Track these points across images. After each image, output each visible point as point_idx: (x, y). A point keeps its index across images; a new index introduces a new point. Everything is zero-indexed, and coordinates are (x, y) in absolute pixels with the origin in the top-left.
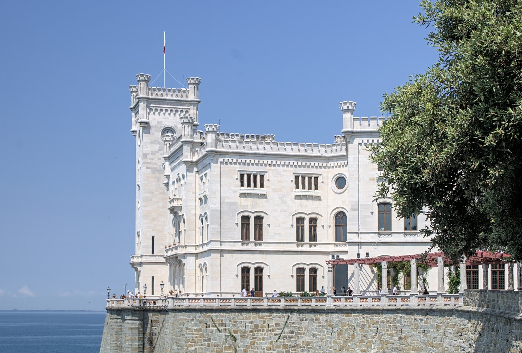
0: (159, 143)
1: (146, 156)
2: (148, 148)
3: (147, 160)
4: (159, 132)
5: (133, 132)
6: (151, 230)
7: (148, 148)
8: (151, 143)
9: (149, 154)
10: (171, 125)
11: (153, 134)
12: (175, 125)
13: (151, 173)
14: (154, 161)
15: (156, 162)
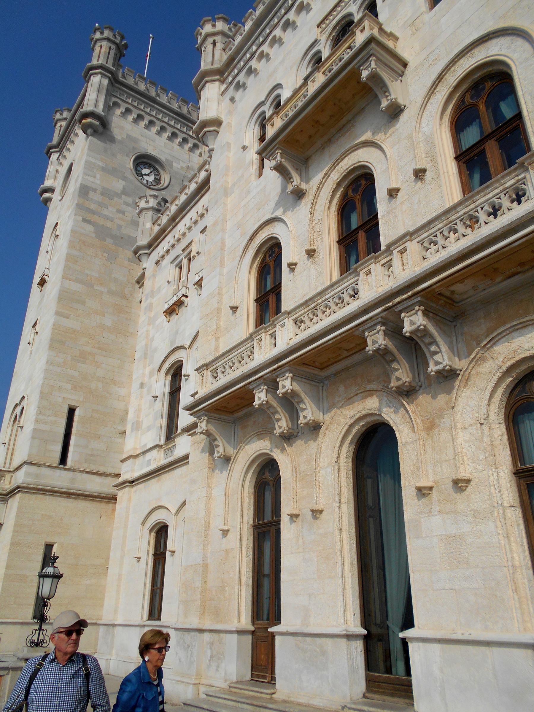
0: (124, 178)
1: (87, 194)
2: (95, 177)
3: (87, 202)
4: (127, 156)
5: (46, 191)
6: (69, 386)
7: (95, 177)
8: (103, 169)
9: (95, 190)
10: (157, 155)
11: (114, 155)
12: (166, 159)
13: (94, 235)
14: (105, 212)
15: (111, 215)
